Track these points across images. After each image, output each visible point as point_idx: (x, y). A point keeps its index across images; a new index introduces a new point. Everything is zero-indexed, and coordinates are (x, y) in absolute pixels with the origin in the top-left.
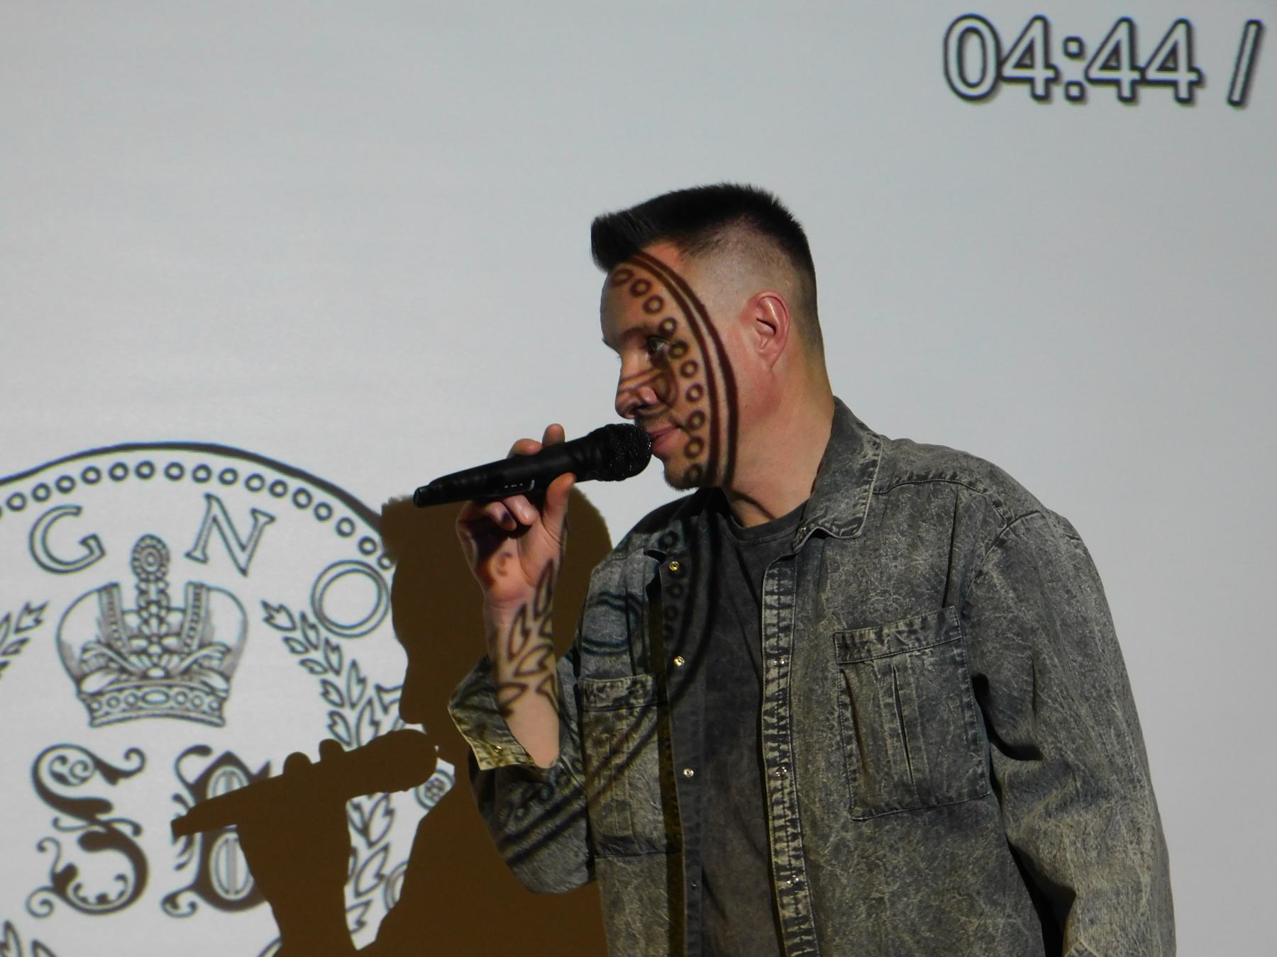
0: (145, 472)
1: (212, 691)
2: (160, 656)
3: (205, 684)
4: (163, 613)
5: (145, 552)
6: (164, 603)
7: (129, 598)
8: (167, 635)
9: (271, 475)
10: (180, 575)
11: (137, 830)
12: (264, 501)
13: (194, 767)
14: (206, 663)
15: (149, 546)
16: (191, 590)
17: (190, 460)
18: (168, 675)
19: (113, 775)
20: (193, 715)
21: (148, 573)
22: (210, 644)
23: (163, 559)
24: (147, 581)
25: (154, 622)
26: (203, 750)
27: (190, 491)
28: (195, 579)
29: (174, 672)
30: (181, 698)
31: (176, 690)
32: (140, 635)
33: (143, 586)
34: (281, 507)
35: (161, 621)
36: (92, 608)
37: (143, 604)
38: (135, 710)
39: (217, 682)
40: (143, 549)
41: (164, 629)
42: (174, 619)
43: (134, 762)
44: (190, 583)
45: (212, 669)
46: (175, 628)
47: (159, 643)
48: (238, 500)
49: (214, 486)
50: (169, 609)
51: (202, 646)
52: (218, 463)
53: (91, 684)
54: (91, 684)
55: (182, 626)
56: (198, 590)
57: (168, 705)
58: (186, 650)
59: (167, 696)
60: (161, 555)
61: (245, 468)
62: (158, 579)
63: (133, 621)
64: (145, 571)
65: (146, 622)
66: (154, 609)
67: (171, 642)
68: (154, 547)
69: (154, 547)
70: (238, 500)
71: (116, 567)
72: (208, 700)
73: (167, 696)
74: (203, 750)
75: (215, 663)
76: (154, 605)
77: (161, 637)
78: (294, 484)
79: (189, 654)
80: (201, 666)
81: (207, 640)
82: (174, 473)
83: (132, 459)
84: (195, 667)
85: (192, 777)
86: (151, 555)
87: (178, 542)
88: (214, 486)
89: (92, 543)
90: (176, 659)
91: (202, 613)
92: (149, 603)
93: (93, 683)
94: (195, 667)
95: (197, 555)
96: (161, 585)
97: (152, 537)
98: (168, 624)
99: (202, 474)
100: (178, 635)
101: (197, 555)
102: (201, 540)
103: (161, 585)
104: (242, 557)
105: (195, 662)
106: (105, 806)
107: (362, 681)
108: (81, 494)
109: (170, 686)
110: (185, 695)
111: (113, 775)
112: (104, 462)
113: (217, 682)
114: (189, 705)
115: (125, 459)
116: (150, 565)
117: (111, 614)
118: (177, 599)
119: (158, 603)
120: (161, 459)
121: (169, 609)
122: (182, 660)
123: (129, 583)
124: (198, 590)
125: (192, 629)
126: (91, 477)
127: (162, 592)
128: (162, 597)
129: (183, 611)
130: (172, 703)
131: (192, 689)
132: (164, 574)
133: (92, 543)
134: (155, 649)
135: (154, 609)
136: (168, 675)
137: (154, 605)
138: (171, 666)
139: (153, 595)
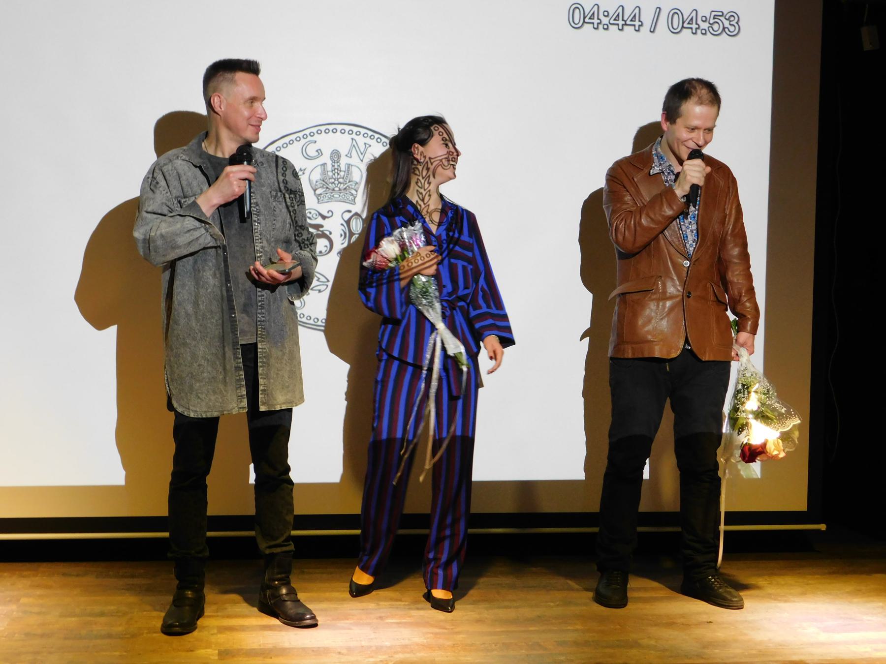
0: (335, 131)
1: (352, 195)
7: (329, 168)
9: (370, 133)
10: (344, 161)
11: (331, 233)
12: (368, 140)
13: (347, 216)
17: (347, 128)
19: (324, 217)
23: (339, 157)
26: (349, 211)
27: (347, 138)
32: (332, 178)
34: (373, 142)
36: (319, 170)
38: (331, 199)
39: (354, 192)
42: (342, 174)
43: (330, 214)
48: (361, 140)
49: (354, 136)
52: (355, 129)
53: (318, 192)
54: (318, 192)
56: (349, 166)
61: (363, 131)
63: (330, 174)
67: (341, 180)
70: (361, 140)
71: (326, 159)
74: (349, 211)
76: (336, 170)
78: (377, 136)
82: (343, 132)
83: (331, 127)
86: (336, 156)
87: (344, 152)
88: (354, 136)
89: (319, 152)
93: (318, 192)
95: (349, 155)
99: (351, 132)
101: (349, 155)
102: (350, 152)
104: (361, 157)
106: (322, 226)
111: (324, 217)
112: (323, 128)
113: (354, 192)
115: (329, 127)
117: (324, 172)
118: (343, 168)
120: (339, 127)
124: (349, 166)
126: (319, 132)
133: (319, 152)
134: (336, 182)
137: (336, 170)
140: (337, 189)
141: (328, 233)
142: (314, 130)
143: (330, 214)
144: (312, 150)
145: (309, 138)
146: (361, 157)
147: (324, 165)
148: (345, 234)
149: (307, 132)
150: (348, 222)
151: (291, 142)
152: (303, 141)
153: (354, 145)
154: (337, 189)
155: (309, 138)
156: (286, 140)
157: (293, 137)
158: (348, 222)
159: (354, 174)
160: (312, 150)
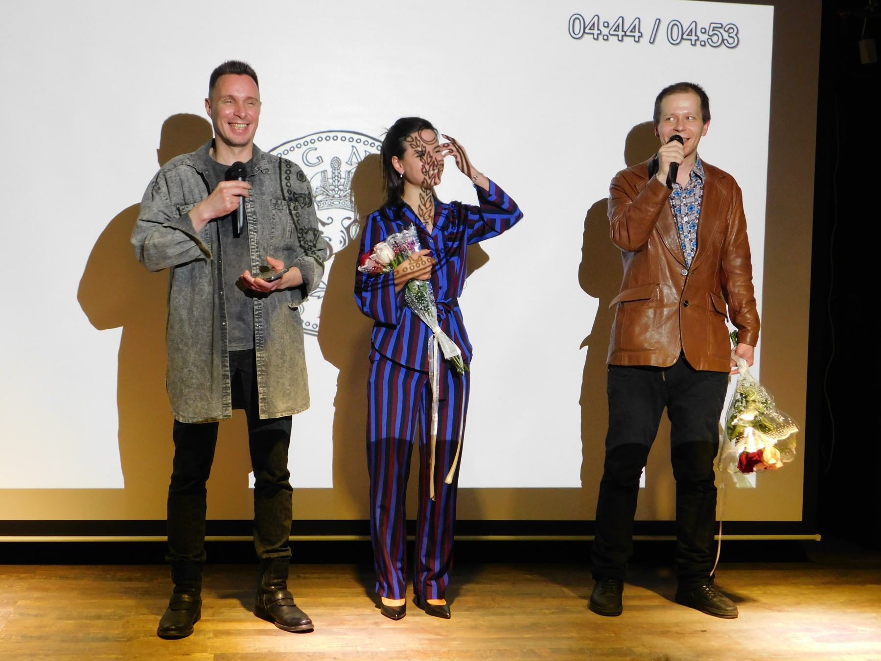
0: (335, 139)
7: (330, 175)
9: (371, 141)
11: (330, 240)
13: (347, 223)
17: (348, 135)
23: (340, 164)
26: (349, 218)
38: (331, 206)
42: (342, 181)
43: (330, 221)
49: (354, 143)
52: (356, 137)
61: (363, 138)
63: (330, 181)
67: (341, 187)
71: (326, 166)
82: (343, 139)
83: (332, 135)
85: (346, 226)
88: (354, 143)
89: (320, 158)
99: (351, 140)
108: (317, 144)
112: (324, 135)
115: (329, 135)
117: (325, 179)
120: (340, 135)
123: (330, 170)
126: (320, 139)
133: (320, 158)
140: (337, 196)
141: (327, 240)
142: (315, 137)
143: (330, 221)
144: (312, 158)
145: (310, 145)
147: (324, 172)
148: (345, 240)
149: (308, 139)
150: (348, 229)
151: (292, 149)
152: (304, 148)
154: (337, 196)
155: (310, 145)
156: (287, 147)
157: (294, 144)
158: (348, 229)
160: (312, 158)
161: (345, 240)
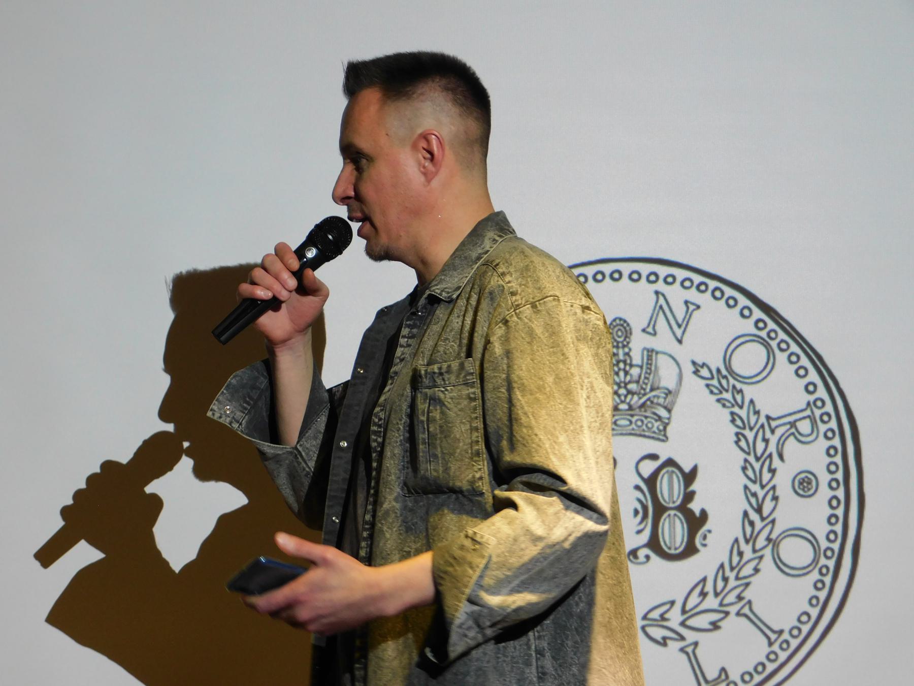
0: (616, 276)
1: (660, 418)
2: (626, 396)
3: (655, 414)
4: (628, 368)
5: (616, 329)
6: (628, 361)
8: (630, 382)
9: (697, 279)
10: (638, 344)
12: (693, 295)
13: (648, 468)
14: (655, 401)
15: (617, 325)
16: (645, 353)
17: (645, 269)
18: (631, 408)
20: (647, 434)
21: (618, 342)
22: (658, 388)
23: (628, 333)
24: (617, 347)
25: (622, 374)
26: (653, 457)
28: (649, 346)
29: (635, 407)
30: (639, 423)
31: (636, 418)
33: (615, 350)
34: (704, 299)
35: (626, 373)
37: (615, 362)
39: (663, 413)
40: (615, 327)
41: (628, 378)
42: (635, 372)
44: (644, 349)
45: (659, 404)
46: (635, 378)
47: (625, 387)
48: (676, 295)
50: (631, 366)
51: (652, 390)
52: (663, 271)
55: (640, 377)
56: (650, 353)
57: (631, 427)
58: (642, 392)
59: (631, 422)
60: (626, 331)
61: (681, 274)
62: (624, 346)
64: (615, 340)
65: (617, 374)
66: (622, 365)
68: (622, 325)
69: (622, 325)
70: (676, 295)
72: (656, 424)
73: (631, 422)
74: (653, 457)
75: (661, 401)
77: (626, 384)
78: (713, 284)
79: (645, 395)
80: (652, 402)
81: (656, 385)
82: (635, 277)
83: (607, 268)
84: (648, 403)
85: (646, 475)
87: (637, 322)
88: (660, 286)
90: (636, 398)
91: (653, 368)
92: (618, 362)
94: (648, 403)
95: (650, 330)
96: (626, 350)
97: (621, 319)
98: (631, 375)
99: (653, 278)
100: (638, 382)
101: (650, 330)
103: (626, 350)
104: (679, 332)
105: (649, 399)
107: (757, 413)
109: (632, 416)
110: (642, 421)
113: (663, 413)
114: (644, 427)
116: (619, 337)
118: (637, 359)
119: (625, 362)
120: (626, 268)
121: (631, 366)
122: (640, 398)
124: (650, 353)
125: (646, 378)
127: (627, 354)
128: (627, 357)
129: (641, 367)
130: (633, 426)
131: (646, 417)
132: (628, 343)
135: (622, 365)
136: (631, 408)
138: (632, 403)
139: (621, 357)
140: (623, 407)
146: (679, 335)
148: (645, 508)
150: (651, 481)
153: (661, 307)
158: (651, 481)
159: (663, 372)
161: (645, 508)
